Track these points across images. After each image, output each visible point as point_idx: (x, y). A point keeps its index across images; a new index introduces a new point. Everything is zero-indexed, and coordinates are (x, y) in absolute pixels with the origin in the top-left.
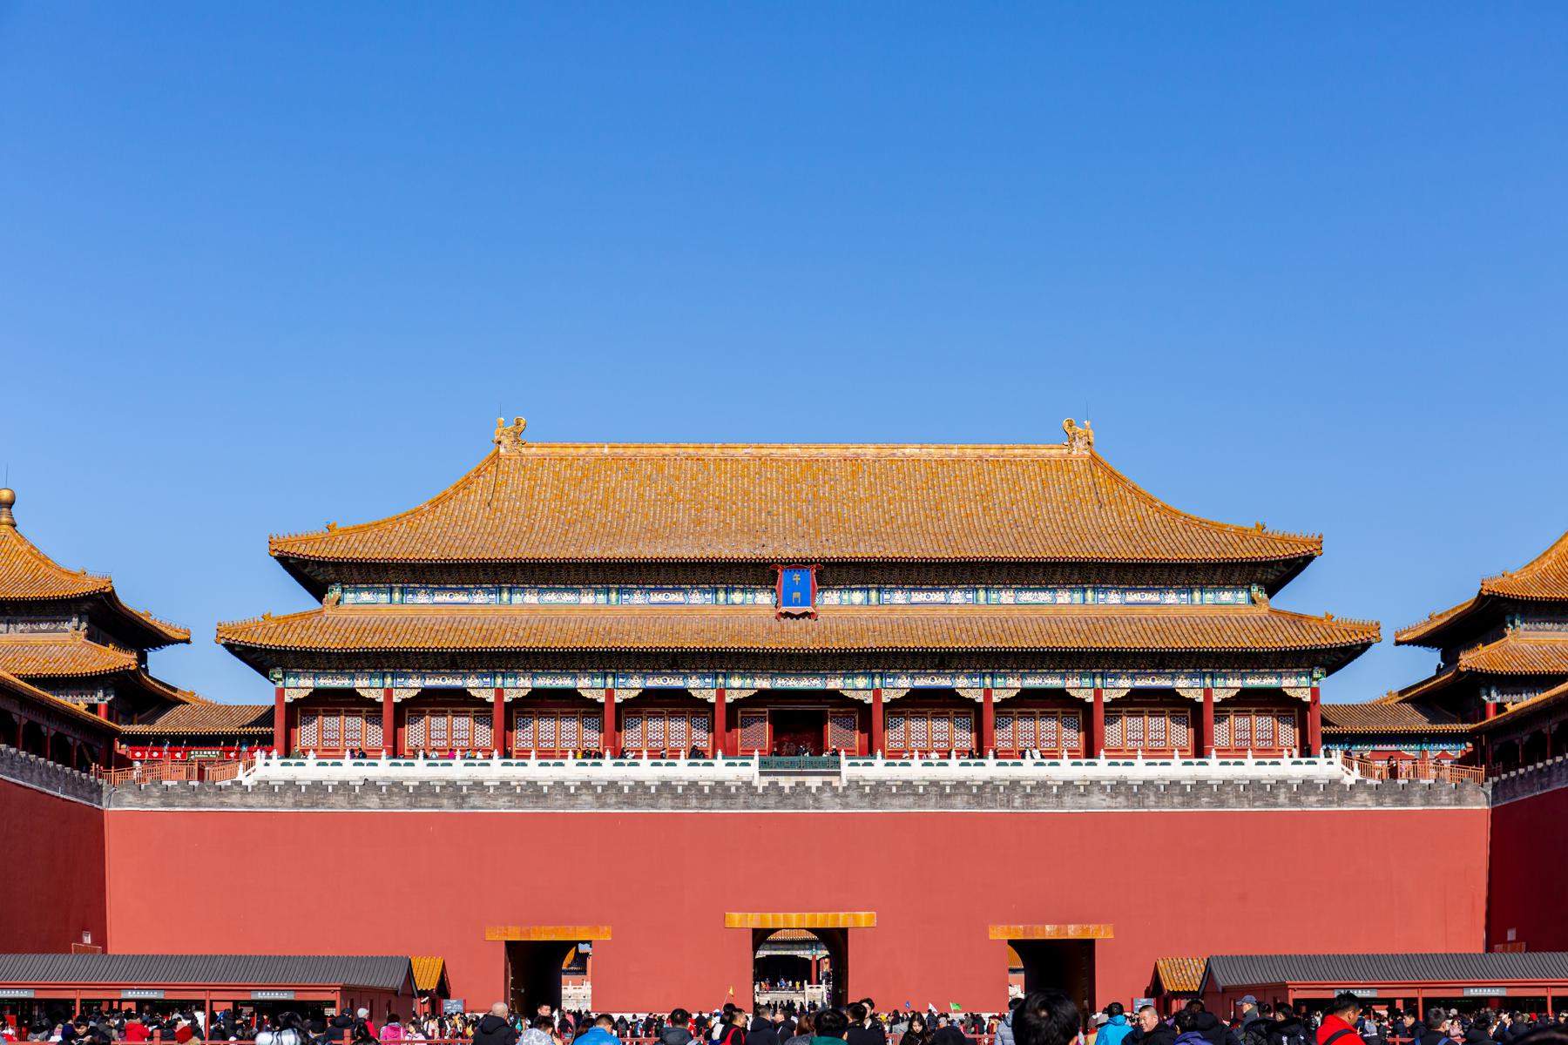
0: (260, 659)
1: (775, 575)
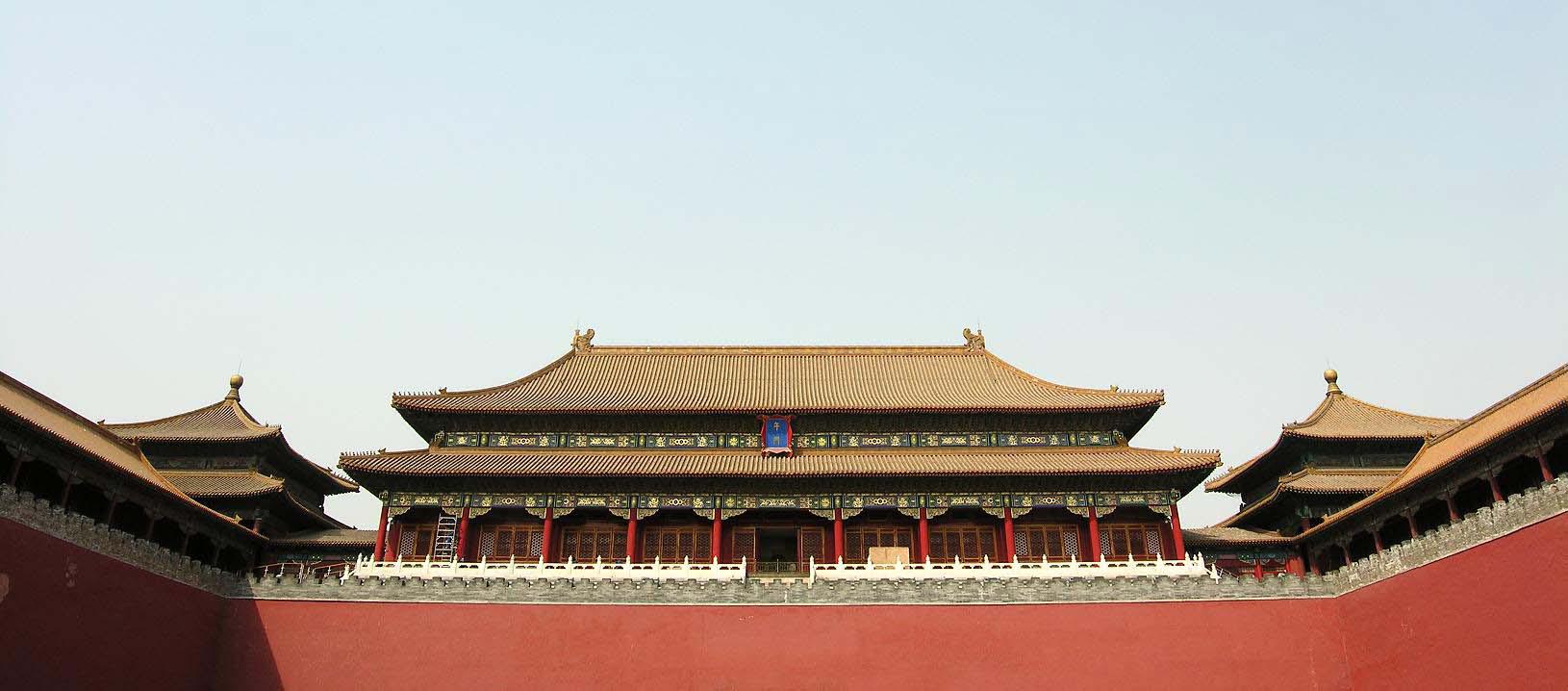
1: (761, 424)
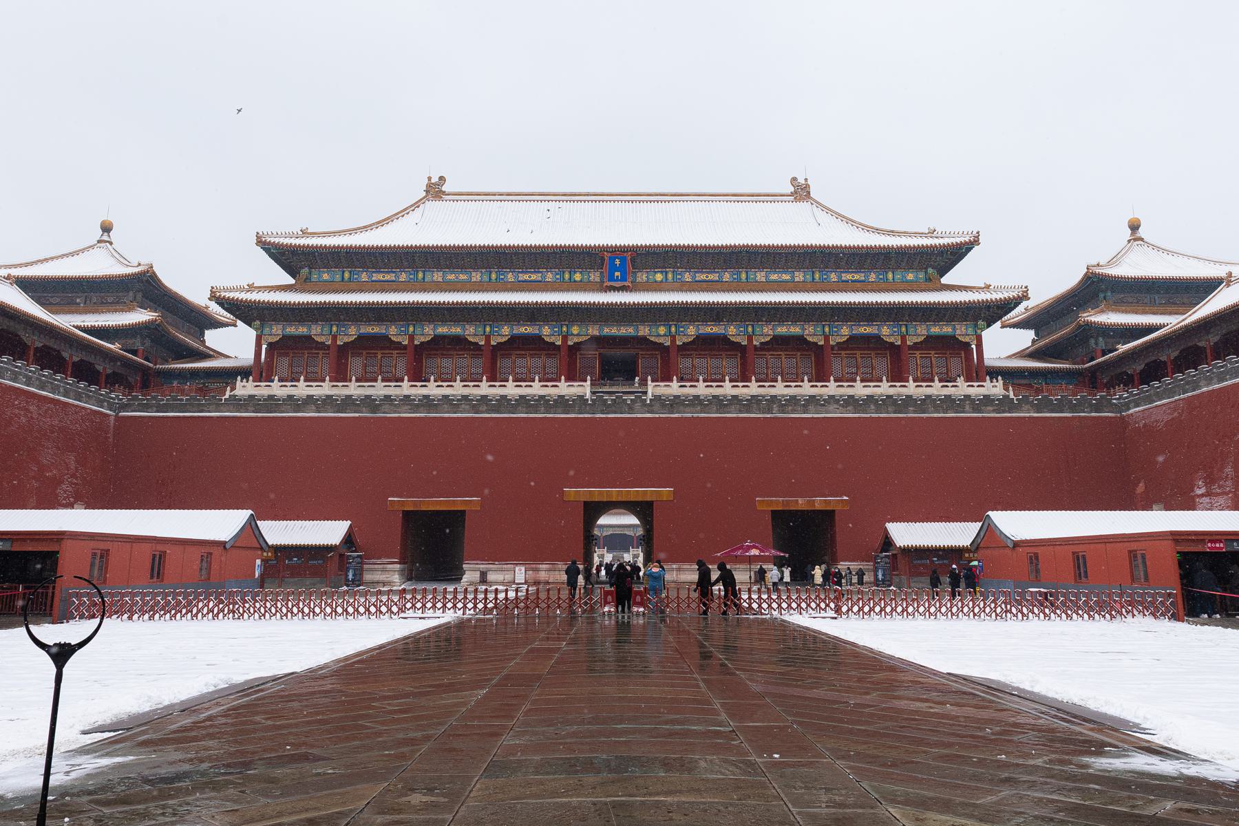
1: (603, 259)
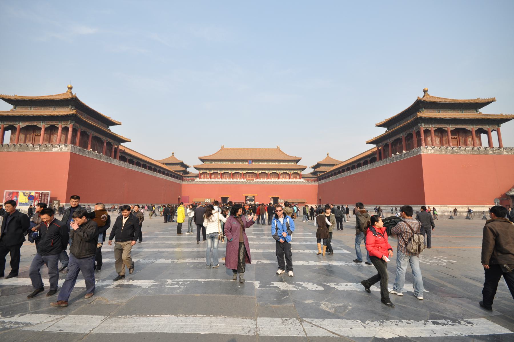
0: (197, 169)
